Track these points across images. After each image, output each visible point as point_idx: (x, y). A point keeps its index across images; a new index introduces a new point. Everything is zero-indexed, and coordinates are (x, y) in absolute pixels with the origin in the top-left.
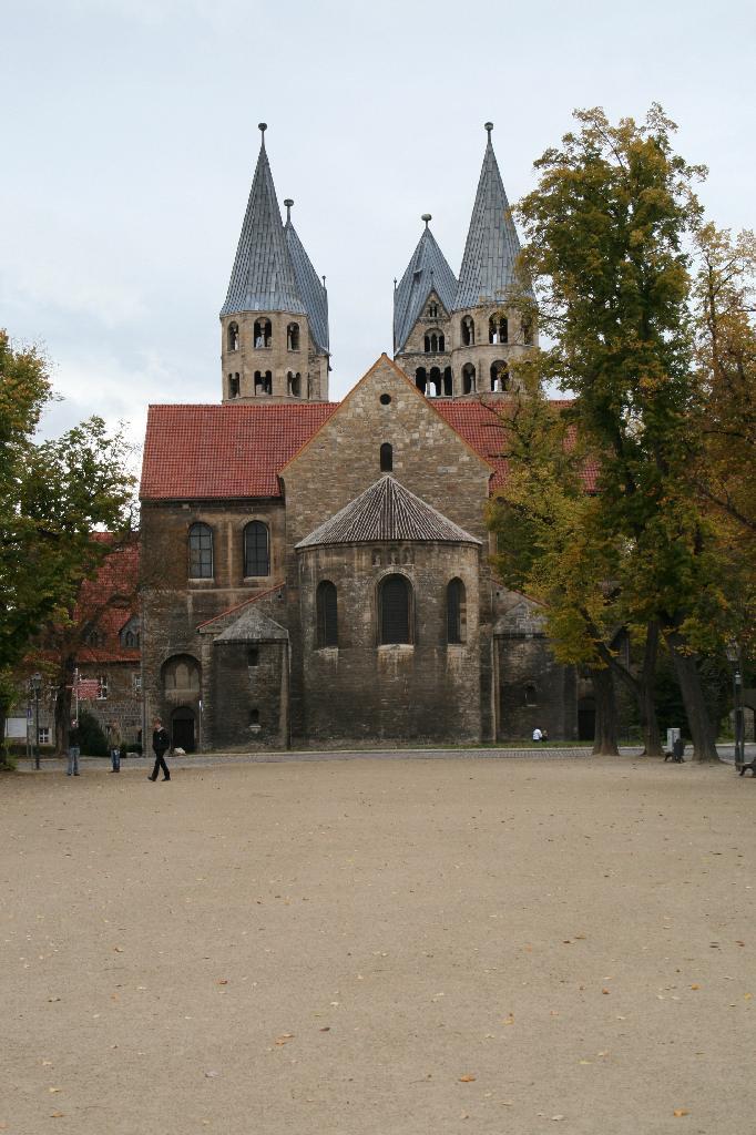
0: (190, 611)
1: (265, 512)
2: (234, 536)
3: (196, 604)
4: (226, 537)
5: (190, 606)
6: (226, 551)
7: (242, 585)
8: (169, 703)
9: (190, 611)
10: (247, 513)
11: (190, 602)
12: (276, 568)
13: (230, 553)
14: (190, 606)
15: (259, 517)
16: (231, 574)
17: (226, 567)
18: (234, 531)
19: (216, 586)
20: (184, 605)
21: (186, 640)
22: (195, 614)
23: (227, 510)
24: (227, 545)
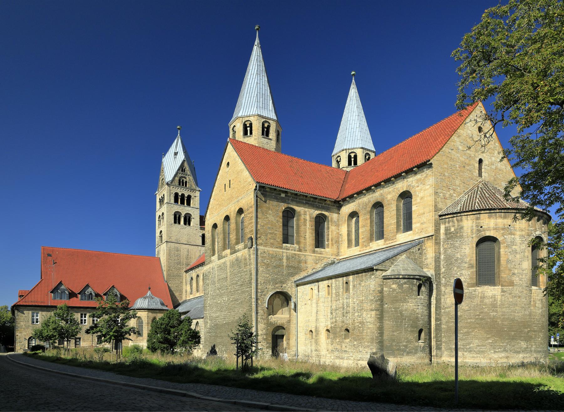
0: (285, 264)
1: (328, 209)
3: (288, 259)
4: (305, 220)
5: (285, 260)
6: (305, 229)
7: (314, 252)
9: (285, 264)
11: (285, 258)
12: (332, 245)
13: (308, 231)
14: (285, 260)
15: (323, 212)
16: (308, 243)
18: (310, 217)
19: (300, 250)
20: (281, 260)
21: (282, 282)
22: (288, 266)
23: (306, 203)
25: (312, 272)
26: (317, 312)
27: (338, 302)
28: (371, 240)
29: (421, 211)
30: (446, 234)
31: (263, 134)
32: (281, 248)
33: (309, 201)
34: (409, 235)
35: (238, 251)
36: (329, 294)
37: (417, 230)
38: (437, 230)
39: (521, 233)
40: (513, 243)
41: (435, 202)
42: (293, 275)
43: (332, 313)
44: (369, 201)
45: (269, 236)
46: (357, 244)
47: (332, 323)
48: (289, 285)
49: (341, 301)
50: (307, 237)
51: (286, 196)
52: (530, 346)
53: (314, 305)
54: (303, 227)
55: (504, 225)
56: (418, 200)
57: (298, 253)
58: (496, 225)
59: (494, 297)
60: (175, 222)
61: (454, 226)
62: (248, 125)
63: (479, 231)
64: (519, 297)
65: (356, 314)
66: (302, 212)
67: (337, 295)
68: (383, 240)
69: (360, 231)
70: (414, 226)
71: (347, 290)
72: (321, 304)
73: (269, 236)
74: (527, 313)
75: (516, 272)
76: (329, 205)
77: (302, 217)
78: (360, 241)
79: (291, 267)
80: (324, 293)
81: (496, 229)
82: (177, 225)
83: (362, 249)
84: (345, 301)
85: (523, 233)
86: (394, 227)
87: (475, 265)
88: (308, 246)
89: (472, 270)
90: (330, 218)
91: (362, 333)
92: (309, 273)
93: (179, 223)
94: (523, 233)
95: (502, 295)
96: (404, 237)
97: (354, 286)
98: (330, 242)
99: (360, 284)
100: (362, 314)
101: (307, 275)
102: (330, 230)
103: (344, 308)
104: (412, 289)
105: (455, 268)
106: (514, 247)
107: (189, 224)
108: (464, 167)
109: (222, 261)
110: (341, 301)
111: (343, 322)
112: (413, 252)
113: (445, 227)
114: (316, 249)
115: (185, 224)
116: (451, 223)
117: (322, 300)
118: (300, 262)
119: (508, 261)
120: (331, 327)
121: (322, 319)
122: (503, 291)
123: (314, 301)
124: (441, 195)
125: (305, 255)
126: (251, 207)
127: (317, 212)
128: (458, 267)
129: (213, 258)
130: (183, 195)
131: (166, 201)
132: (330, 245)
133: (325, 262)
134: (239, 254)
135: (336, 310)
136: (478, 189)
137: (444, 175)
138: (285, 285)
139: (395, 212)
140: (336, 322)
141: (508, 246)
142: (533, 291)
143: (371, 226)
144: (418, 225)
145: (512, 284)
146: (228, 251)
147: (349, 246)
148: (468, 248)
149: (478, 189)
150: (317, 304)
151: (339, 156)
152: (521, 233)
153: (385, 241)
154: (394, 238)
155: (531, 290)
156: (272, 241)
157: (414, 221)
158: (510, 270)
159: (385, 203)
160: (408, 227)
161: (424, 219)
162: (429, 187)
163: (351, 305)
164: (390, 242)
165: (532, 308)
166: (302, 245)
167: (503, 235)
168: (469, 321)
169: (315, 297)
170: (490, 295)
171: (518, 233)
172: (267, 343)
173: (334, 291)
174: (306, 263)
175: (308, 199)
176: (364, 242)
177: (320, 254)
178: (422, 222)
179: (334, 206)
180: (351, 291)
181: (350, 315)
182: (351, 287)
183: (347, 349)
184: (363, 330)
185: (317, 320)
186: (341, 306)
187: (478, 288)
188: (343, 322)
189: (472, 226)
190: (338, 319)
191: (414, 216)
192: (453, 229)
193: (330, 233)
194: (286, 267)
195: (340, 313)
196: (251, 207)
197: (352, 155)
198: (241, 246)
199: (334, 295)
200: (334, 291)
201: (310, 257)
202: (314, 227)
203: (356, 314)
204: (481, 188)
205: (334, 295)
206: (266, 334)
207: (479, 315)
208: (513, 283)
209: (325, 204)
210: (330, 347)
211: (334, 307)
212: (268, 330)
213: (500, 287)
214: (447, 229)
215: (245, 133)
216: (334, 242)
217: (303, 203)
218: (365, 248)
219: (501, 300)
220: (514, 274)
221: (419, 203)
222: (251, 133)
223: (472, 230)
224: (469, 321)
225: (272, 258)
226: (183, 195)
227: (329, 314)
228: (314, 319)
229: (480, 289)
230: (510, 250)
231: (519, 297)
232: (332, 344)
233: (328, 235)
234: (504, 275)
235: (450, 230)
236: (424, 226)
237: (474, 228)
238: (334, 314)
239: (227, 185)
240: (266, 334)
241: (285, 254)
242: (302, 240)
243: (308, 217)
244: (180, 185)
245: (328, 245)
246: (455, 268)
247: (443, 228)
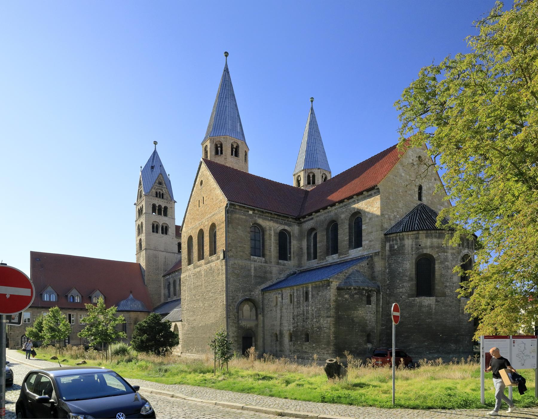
0: (253, 274)
1: (289, 225)
2: (275, 236)
3: (255, 269)
4: (270, 235)
5: (253, 271)
6: (270, 243)
7: (278, 264)
9: (253, 274)
10: (281, 224)
11: (253, 269)
12: (294, 257)
13: (272, 245)
14: (253, 271)
15: (286, 228)
16: (273, 256)
17: (270, 251)
18: (275, 232)
19: (266, 262)
20: (249, 270)
21: (251, 291)
22: (255, 276)
23: (271, 220)
24: (271, 240)
25: (277, 281)
26: (281, 317)
27: (299, 309)
28: (328, 254)
29: (370, 230)
30: (390, 251)
31: (232, 154)
32: (250, 260)
33: (274, 218)
34: (359, 251)
35: (212, 261)
36: (291, 302)
37: (366, 247)
38: (383, 247)
40: (446, 260)
41: (382, 223)
42: (260, 284)
43: (294, 319)
44: (326, 220)
45: (239, 249)
46: (315, 258)
47: (294, 328)
48: (257, 293)
49: (302, 309)
50: (272, 250)
51: (253, 213)
52: (458, 348)
53: (278, 311)
54: (268, 241)
55: (439, 244)
56: (367, 221)
57: (264, 264)
58: (432, 244)
59: (429, 306)
60: (153, 232)
61: (397, 244)
62: (219, 145)
63: (418, 249)
64: (450, 306)
65: (315, 320)
66: (268, 228)
67: (298, 303)
68: (337, 255)
69: (318, 245)
70: (364, 243)
71: (307, 299)
72: (284, 311)
73: (239, 249)
74: (456, 319)
75: (448, 285)
76: (291, 221)
77: (267, 233)
78: (318, 255)
79: (259, 277)
80: (287, 300)
81: (432, 247)
82: (155, 234)
83: (319, 262)
84: (305, 308)
85: (454, 251)
86: (346, 243)
87: (414, 278)
88: (272, 258)
89: (412, 283)
91: (319, 337)
92: (274, 282)
93: (157, 232)
94: (454, 251)
95: (436, 305)
96: (354, 253)
97: (313, 295)
98: (292, 255)
99: (318, 294)
100: (319, 321)
101: (271, 284)
102: (292, 244)
103: (304, 314)
104: (361, 299)
105: (398, 281)
106: (446, 263)
107: (166, 234)
108: (406, 192)
109: (198, 269)
110: (302, 309)
111: (303, 326)
112: (362, 266)
113: (390, 245)
114: (281, 261)
115: (162, 233)
116: (394, 242)
117: (285, 307)
118: (265, 272)
119: (442, 275)
120: (293, 331)
121: (285, 324)
122: (437, 301)
123: (279, 308)
124: (387, 216)
125: (270, 267)
126: (223, 222)
127: (282, 227)
128: (400, 280)
129: (189, 267)
130: (160, 206)
131: (144, 211)
132: (292, 258)
133: (287, 272)
134: (213, 264)
135: (297, 316)
136: (417, 211)
137: (389, 199)
138: (253, 293)
139: (347, 230)
140: (297, 326)
141: (442, 263)
143: (327, 242)
144: (367, 242)
145: (444, 295)
146: (202, 262)
147: (309, 259)
148: (408, 264)
149: (417, 211)
150: (281, 310)
151: (299, 176)
153: (339, 256)
154: (347, 253)
156: (241, 253)
157: (363, 238)
158: (443, 283)
159: (339, 222)
160: (358, 244)
161: (372, 237)
162: (376, 209)
163: (310, 312)
164: (343, 256)
165: (461, 316)
166: (267, 257)
167: (438, 252)
168: (409, 326)
169: (279, 304)
170: (426, 304)
171: (450, 251)
172: (238, 344)
173: (296, 300)
174: (271, 273)
175: (273, 216)
176: (321, 255)
177: (283, 265)
178: (371, 239)
179: (295, 222)
180: (310, 300)
181: (309, 321)
182: (310, 296)
183: (307, 350)
184: (321, 334)
185: (281, 324)
186: (301, 312)
187: (416, 298)
188: (303, 326)
189: (412, 245)
190: (299, 324)
191: (364, 234)
192: (396, 247)
193: (292, 247)
194: (254, 276)
195: (300, 318)
196: (223, 222)
197: (311, 176)
198: (214, 257)
199: (295, 303)
200: (296, 300)
202: (278, 242)
203: (315, 320)
204: (420, 211)
205: (295, 303)
206: (237, 337)
207: (417, 322)
208: (445, 294)
209: (288, 221)
210: (293, 348)
211: (295, 313)
212: (238, 332)
213: (434, 298)
214: (391, 247)
215: (217, 153)
217: (268, 220)
218: (322, 261)
219: (435, 308)
220: (446, 286)
221: (368, 223)
222: (222, 153)
223: (412, 248)
224: (409, 326)
225: (242, 268)
226: (160, 206)
227: (292, 320)
228: (279, 323)
229: (418, 299)
230: (443, 266)
232: (294, 346)
233: (290, 249)
234: (438, 287)
235: (394, 247)
236: (372, 243)
237: (414, 246)
238: (295, 319)
239: (201, 202)
240: (237, 337)
241: (252, 266)
242: (267, 252)
244: (157, 196)
245: (290, 257)
246: (398, 281)
247: (388, 245)
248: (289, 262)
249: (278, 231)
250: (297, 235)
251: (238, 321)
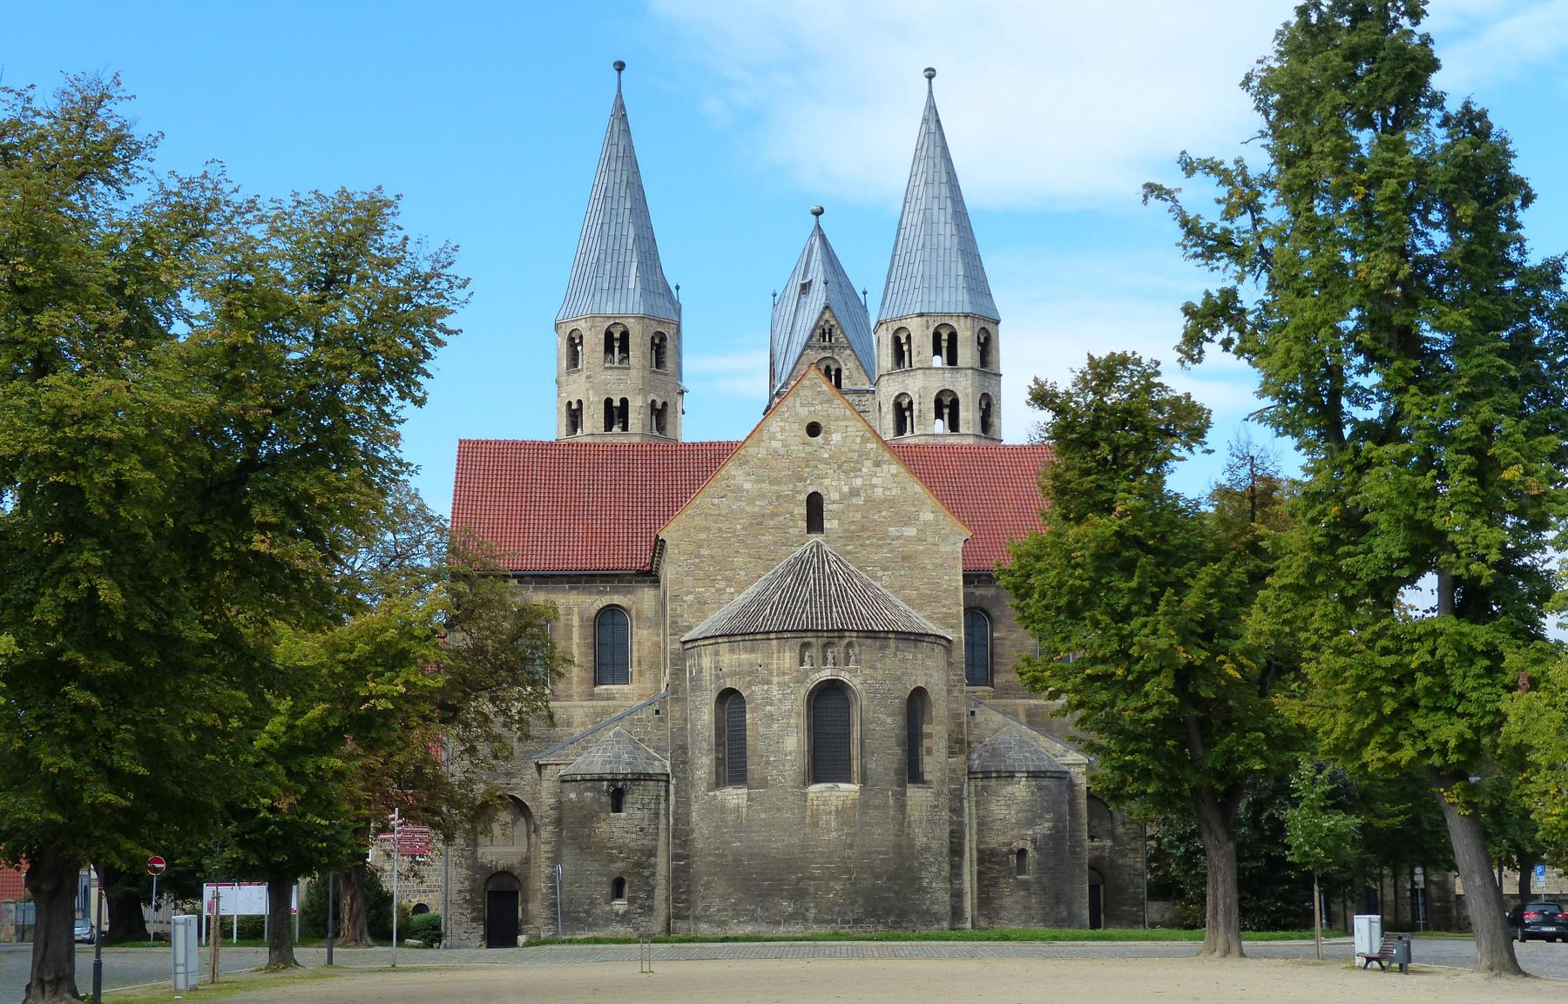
4: (569, 627)
8: (482, 866)
12: (641, 673)
15: (617, 599)
39: (781, 679)
59: (738, 808)
64: (778, 810)
90: (633, 613)
94: (787, 678)
95: (749, 807)
112: (640, 720)
138: (514, 781)
142: (810, 796)
145: (764, 783)
152: (781, 679)
155: (806, 795)
165: (808, 830)
174: (569, 724)
201: (580, 711)
202: (591, 640)
208: (766, 780)
213: (745, 791)
216: (644, 667)
220: (768, 763)
231: (778, 810)
243: (576, 621)
248: (626, 687)
249: (593, 612)
250: (651, 615)
251: (474, 852)
